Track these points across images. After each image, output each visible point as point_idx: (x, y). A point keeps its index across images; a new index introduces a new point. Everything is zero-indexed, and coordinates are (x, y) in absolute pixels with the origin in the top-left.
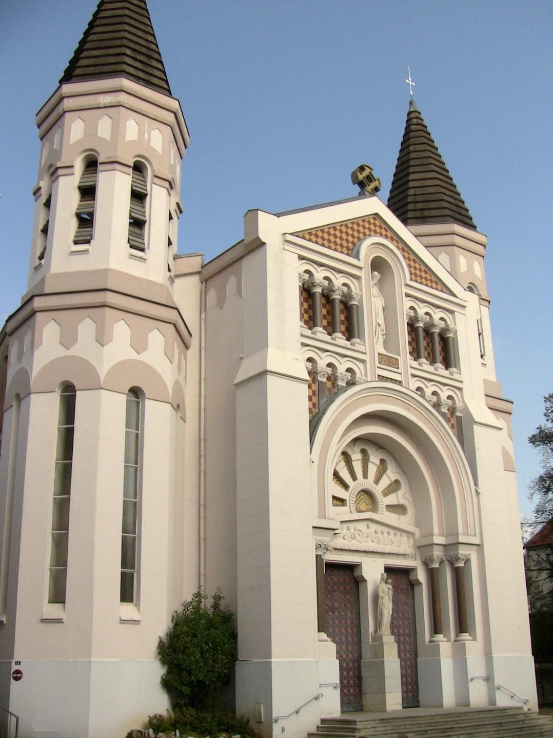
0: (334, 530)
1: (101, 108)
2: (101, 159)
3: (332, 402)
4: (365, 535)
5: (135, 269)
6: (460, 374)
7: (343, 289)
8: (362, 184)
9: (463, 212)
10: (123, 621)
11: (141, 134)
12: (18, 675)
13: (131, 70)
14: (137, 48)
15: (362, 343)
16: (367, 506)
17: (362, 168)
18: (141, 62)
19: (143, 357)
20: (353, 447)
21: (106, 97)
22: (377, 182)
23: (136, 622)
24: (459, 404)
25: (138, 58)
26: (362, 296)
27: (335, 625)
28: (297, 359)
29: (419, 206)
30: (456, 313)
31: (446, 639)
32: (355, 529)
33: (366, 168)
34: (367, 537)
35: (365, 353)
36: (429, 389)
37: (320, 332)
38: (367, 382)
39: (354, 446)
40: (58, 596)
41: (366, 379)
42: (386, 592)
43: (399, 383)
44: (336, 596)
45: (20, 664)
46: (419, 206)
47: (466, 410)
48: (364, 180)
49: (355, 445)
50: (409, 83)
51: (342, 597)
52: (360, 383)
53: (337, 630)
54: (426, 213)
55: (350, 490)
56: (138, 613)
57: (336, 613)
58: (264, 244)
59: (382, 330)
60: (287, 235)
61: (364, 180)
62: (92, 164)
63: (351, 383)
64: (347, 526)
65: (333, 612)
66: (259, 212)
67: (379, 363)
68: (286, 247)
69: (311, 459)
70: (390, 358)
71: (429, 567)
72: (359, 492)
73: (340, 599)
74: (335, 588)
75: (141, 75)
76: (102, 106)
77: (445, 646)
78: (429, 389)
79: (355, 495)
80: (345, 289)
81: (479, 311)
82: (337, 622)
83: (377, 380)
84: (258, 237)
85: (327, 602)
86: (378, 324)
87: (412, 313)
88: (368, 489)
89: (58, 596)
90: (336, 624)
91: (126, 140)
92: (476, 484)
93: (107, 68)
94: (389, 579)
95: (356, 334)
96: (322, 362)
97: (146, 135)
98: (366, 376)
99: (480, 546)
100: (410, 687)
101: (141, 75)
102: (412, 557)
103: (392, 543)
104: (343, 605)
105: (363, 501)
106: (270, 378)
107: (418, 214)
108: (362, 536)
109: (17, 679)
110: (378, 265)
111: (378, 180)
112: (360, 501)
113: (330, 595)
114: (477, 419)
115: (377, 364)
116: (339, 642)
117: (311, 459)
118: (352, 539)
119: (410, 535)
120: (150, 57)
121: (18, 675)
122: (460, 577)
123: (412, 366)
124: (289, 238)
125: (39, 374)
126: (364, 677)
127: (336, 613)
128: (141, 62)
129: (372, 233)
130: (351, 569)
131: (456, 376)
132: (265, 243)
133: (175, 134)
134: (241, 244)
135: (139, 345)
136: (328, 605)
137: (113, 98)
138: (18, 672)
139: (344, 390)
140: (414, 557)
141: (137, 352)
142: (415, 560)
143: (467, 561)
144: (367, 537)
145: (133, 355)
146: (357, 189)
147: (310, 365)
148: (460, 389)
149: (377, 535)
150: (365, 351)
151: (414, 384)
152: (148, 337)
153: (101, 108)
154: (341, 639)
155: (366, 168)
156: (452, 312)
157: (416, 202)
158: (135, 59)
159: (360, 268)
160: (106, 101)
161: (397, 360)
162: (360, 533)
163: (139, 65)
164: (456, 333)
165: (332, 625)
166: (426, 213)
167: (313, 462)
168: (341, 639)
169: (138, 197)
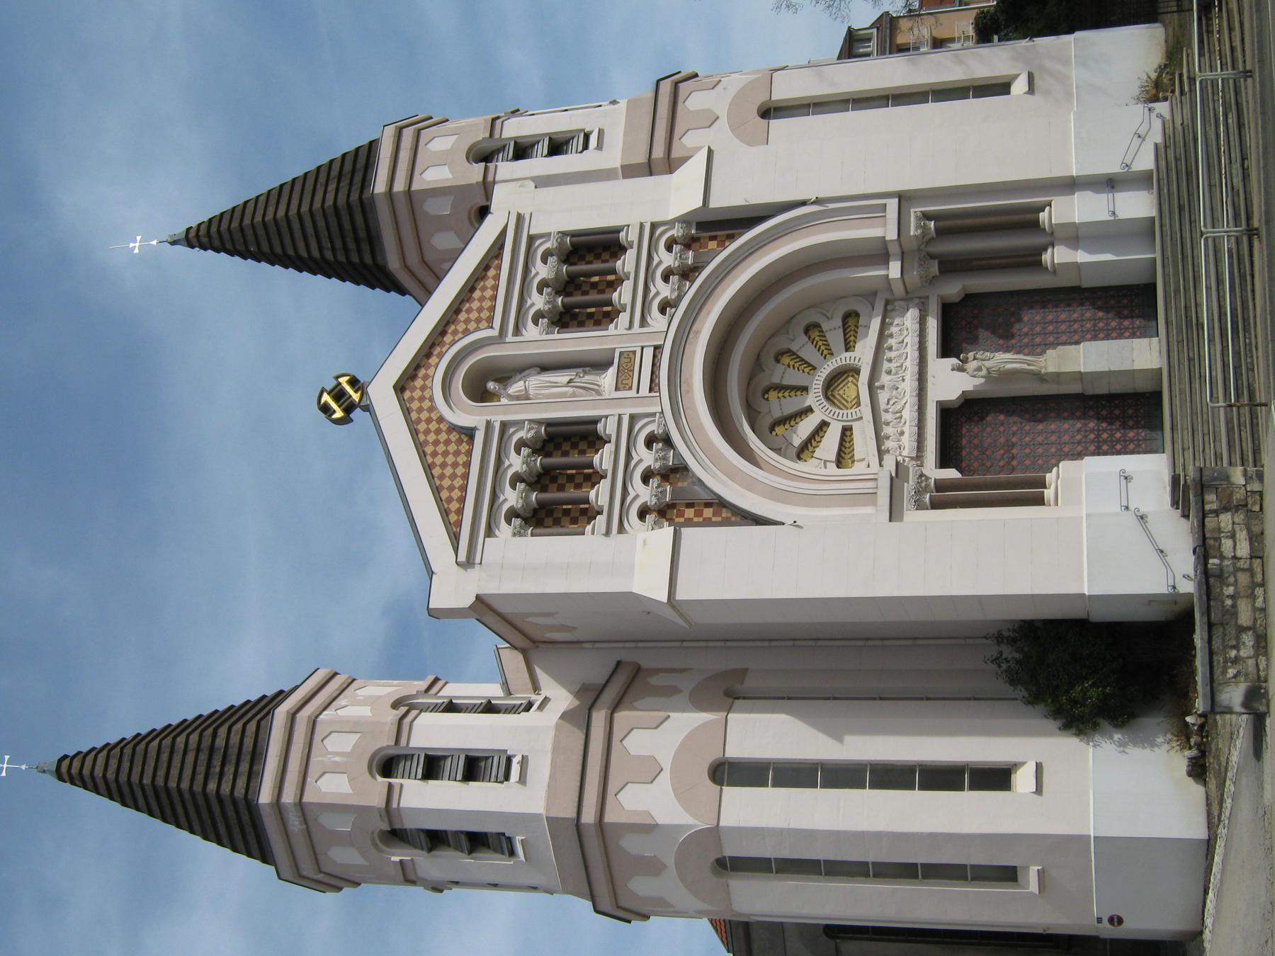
0: (892, 478)
1: (307, 827)
2: (386, 827)
3: (700, 480)
4: (894, 392)
5: (541, 770)
6: (628, 226)
7: (526, 454)
8: (349, 409)
9: (348, 166)
10: (1039, 790)
11: (336, 770)
12: (1116, 920)
13: (241, 782)
14: (201, 769)
15: (603, 420)
16: (849, 384)
17: (326, 409)
18: (223, 765)
19: (666, 761)
20: (762, 414)
21: (291, 822)
22: (341, 380)
23: (1039, 767)
24: (677, 232)
25: (218, 769)
26: (531, 421)
27: (1032, 443)
28: (644, 542)
29: (351, 245)
30: (530, 233)
31: (1047, 209)
32: (887, 411)
33: (322, 402)
34: (897, 388)
35: (620, 415)
36: (664, 290)
37: (599, 494)
38: (662, 412)
39: (759, 412)
40: (1009, 875)
41: (658, 415)
42: (980, 364)
43: (658, 349)
44: (989, 441)
45: (1101, 918)
46: (351, 245)
47: (684, 220)
48: (344, 406)
49: (759, 410)
50: (140, 245)
51: (989, 429)
52: (666, 425)
53: (1040, 439)
54: (362, 234)
55: (827, 419)
56: (1026, 765)
57: (1014, 440)
58: (478, 597)
59: (577, 375)
60: (458, 560)
61: (344, 406)
62: (397, 835)
63: (668, 441)
64: (883, 413)
65: (1013, 445)
66: (430, 607)
67: (630, 388)
68: (478, 560)
69: (791, 525)
70: (621, 368)
71: (935, 236)
72: (827, 398)
73: (993, 434)
74: (976, 441)
75: (244, 767)
76: (304, 827)
77: (1059, 255)
78: (664, 290)
79: (838, 411)
80: (525, 451)
81: (520, 183)
82: (1027, 439)
83: (658, 394)
84: (470, 607)
85: (998, 457)
86: (569, 382)
87: (543, 322)
88: (825, 379)
89: (1009, 875)
90: (1030, 441)
91: (351, 792)
92: (803, 203)
93: (246, 818)
94: (960, 357)
95: (590, 427)
96: (643, 494)
97: (337, 759)
98: (653, 415)
99: (904, 198)
100: (1125, 301)
101: (244, 767)
102: (923, 303)
103: (901, 366)
104: (1002, 429)
105: (841, 392)
106: (681, 595)
107: (365, 247)
108: (896, 398)
109: (1120, 921)
110: (479, 392)
111: (337, 378)
112: (842, 397)
113: (989, 452)
114: (698, 203)
115: (633, 393)
116: (1057, 434)
117: (791, 525)
118: (901, 417)
119: (889, 307)
120: (212, 749)
121: (1116, 920)
122: (950, 226)
123: (627, 327)
124: (462, 557)
125: (694, 815)
126: (1109, 390)
127: (1014, 440)
128: (223, 765)
129: (427, 394)
130: (948, 414)
131: (633, 236)
132: (477, 595)
133: (323, 706)
134: (484, 621)
135: (649, 771)
136: (1003, 455)
137: (291, 814)
138: (1111, 920)
139: (678, 455)
140: (922, 300)
141: (660, 773)
142: (927, 297)
143: (927, 216)
144: (897, 388)
145: (665, 777)
146: (357, 414)
147: (650, 518)
148: (654, 226)
149: (893, 371)
150: (617, 418)
151: (658, 321)
152: (639, 757)
153: (307, 827)
154: (1053, 432)
155: (322, 402)
156: (532, 239)
157: (346, 250)
158: (221, 774)
159: (489, 425)
160: (297, 823)
161: (621, 353)
162: (891, 402)
163: (230, 769)
164: (565, 234)
165: (1032, 447)
166: (362, 234)
167: (795, 522)
168: (1053, 432)
169: (433, 767)
